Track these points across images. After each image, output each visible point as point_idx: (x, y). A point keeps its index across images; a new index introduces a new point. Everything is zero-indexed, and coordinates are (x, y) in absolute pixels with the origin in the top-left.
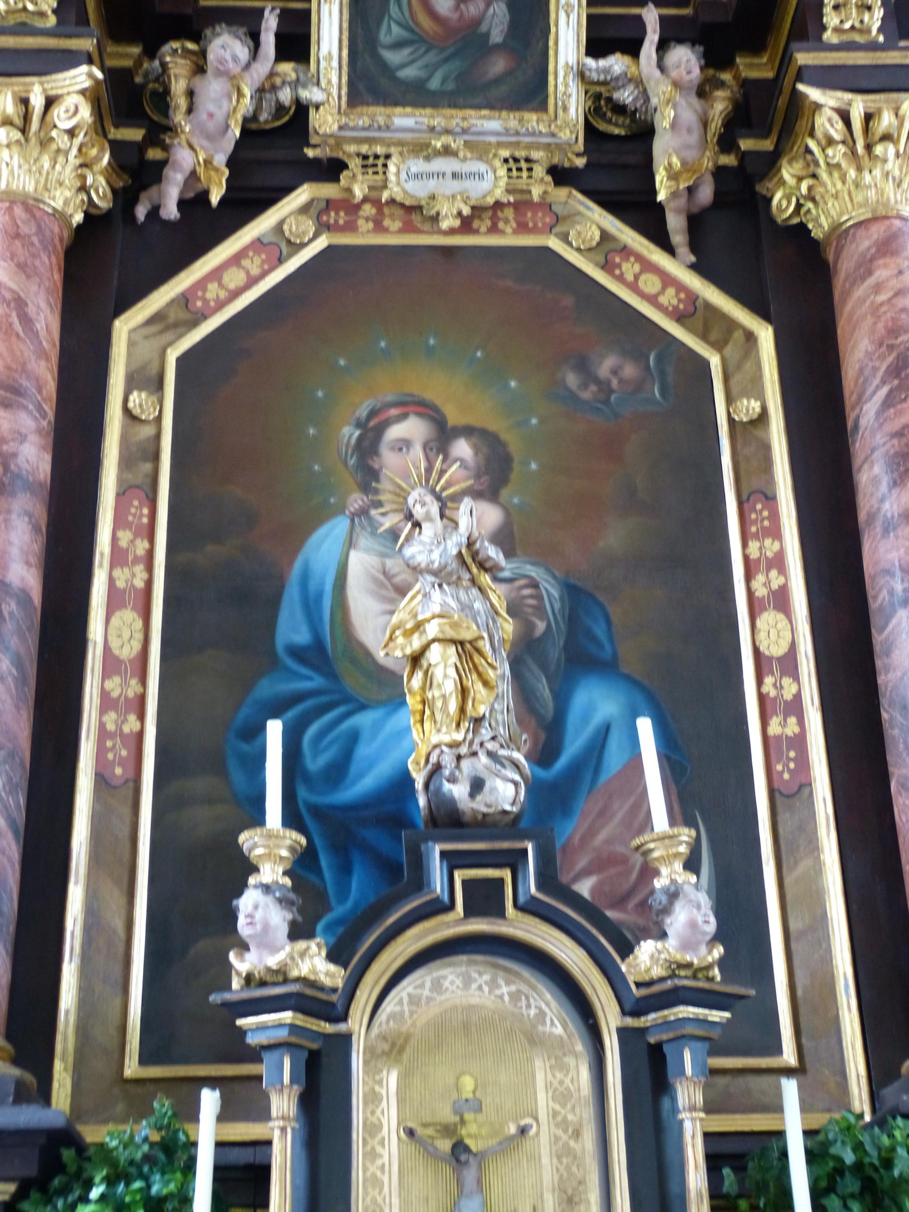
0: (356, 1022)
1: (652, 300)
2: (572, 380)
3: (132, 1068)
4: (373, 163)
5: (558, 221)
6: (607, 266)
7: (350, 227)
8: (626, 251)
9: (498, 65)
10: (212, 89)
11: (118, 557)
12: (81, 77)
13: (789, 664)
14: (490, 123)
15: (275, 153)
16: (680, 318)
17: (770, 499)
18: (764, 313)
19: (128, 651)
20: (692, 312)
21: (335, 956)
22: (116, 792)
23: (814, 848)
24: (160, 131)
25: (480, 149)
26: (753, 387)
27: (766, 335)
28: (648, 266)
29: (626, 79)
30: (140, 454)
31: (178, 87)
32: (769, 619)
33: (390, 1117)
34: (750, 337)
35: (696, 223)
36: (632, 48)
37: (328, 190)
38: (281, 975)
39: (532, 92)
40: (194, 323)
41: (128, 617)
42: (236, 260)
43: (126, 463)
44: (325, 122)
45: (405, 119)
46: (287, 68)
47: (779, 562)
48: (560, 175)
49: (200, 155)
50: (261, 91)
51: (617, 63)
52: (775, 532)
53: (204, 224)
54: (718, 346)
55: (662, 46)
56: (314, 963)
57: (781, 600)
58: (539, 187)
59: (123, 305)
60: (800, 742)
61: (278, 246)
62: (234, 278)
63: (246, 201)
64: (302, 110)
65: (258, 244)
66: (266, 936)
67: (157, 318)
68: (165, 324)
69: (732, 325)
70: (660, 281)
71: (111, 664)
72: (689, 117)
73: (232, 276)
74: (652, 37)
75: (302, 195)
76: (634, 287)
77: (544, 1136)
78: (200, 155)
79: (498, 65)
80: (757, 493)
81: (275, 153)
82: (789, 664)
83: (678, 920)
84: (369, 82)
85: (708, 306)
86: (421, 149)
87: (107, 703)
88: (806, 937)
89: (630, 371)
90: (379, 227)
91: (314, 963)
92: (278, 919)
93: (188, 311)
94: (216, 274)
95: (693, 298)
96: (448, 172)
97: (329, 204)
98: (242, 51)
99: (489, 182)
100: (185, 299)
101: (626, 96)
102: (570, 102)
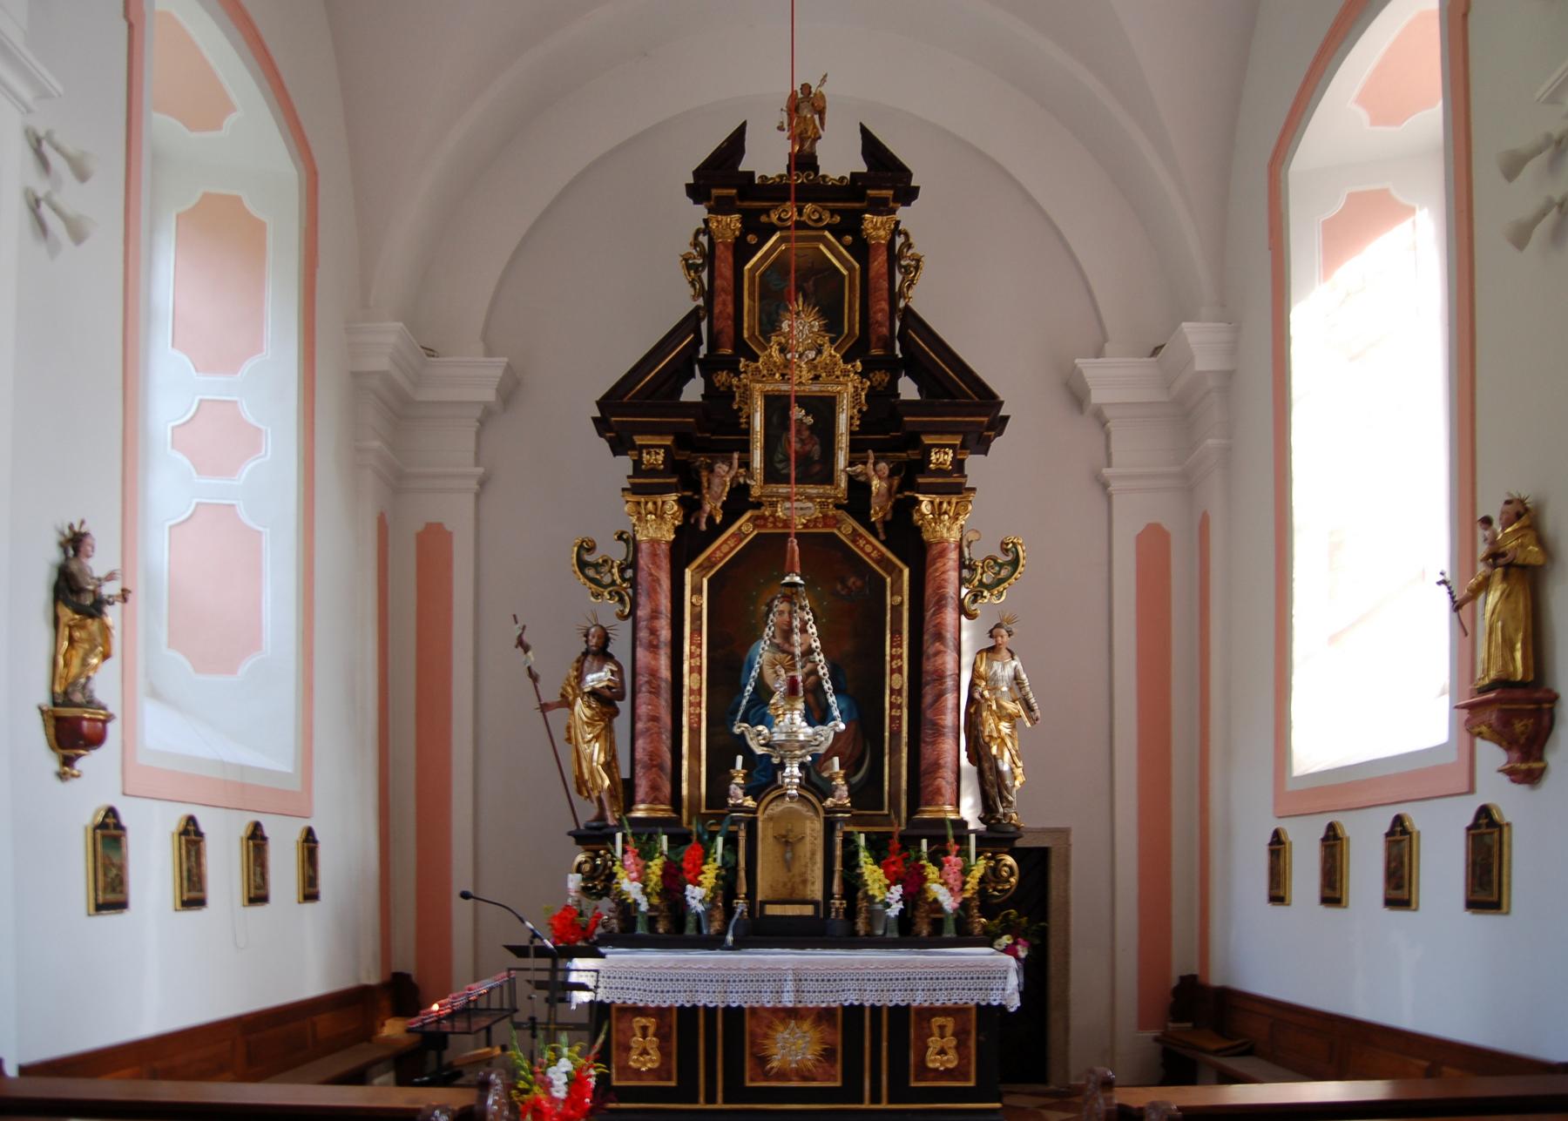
0: (759, 815)
1: (868, 555)
2: (839, 587)
3: (703, 810)
4: (773, 505)
5: (838, 522)
6: (854, 541)
7: (765, 526)
8: (861, 536)
9: (817, 468)
10: (716, 481)
11: (692, 655)
12: (672, 497)
13: (899, 692)
14: (812, 490)
15: (739, 501)
16: (878, 562)
17: (901, 634)
18: (907, 564)
19: (695, 687)
20: (882, 561)
21: (754, 799)
22: (694, 732)
23: (900, 751)
24: (697, 487)
25: (810, 498)
26: (898, 597)
27: (906, 572)
28: (868, 542)
29: (860, 474)
30: (696, 617)
31: (704, 480)
32: (896, 676)
33: (770, 833)
34: (901, 571)
35: (886, 524)
36: (865, 463)
37: (757, 512)
38: (740, 805)
39: (828, 477)
40: (712, 567)
41: (695, 675)
42: (725, 542)
43: (692, 622)
44: (756, 492)
45: (783, 489)
46: (742, 470)
47: (900, 657)
48: (838, 507)
49: (713, 505)
50: (732, 480)
51: (859, 468)
52: (900, 646)
53: (715, 531)
54: (890, 574)
55: (875, 464)
56: (750, 802)
57: (900, 670)
58: (832, 512)
59: (687, 564)
60: (900, 718)
61: (739, 536)
62: (725, 549)
63: (729, 520)
64: (746, 487)
65: (733, 535)
66: (738, 796)
67: (700, 566)
68: (703, 568)
69: (895, 566)
70: (871, 548)
71: (691, 692)
72: (885, 485)
73: (724, 548)
74: (871, 461)
75: (747, 515)
76: (862, 549)
77: (808, 839)
78: (713, 505)
79: (817, 468)
80: (897, 632)
81: (739, 501)
82: (899, 692)
83: (837, 793)
84: (773, 475)
85: (888, 560)
86: (788, 498)
87: (691, 704)
88: (895, 777)
89: (859, 583)
90: (775, 526)
91: (750, 802)
92: (740, 792)
93: (709, 564)
94: (719, 548)
95: (882, 555)
96: (798, 508)
97: (758, 517)
98: (726, 468)
99: (813, 510)
100: (708, 558)
101: (862, 478)
102: (843, 484)
